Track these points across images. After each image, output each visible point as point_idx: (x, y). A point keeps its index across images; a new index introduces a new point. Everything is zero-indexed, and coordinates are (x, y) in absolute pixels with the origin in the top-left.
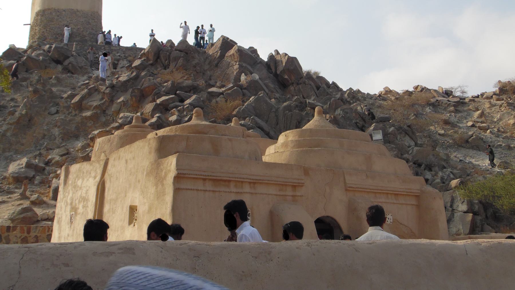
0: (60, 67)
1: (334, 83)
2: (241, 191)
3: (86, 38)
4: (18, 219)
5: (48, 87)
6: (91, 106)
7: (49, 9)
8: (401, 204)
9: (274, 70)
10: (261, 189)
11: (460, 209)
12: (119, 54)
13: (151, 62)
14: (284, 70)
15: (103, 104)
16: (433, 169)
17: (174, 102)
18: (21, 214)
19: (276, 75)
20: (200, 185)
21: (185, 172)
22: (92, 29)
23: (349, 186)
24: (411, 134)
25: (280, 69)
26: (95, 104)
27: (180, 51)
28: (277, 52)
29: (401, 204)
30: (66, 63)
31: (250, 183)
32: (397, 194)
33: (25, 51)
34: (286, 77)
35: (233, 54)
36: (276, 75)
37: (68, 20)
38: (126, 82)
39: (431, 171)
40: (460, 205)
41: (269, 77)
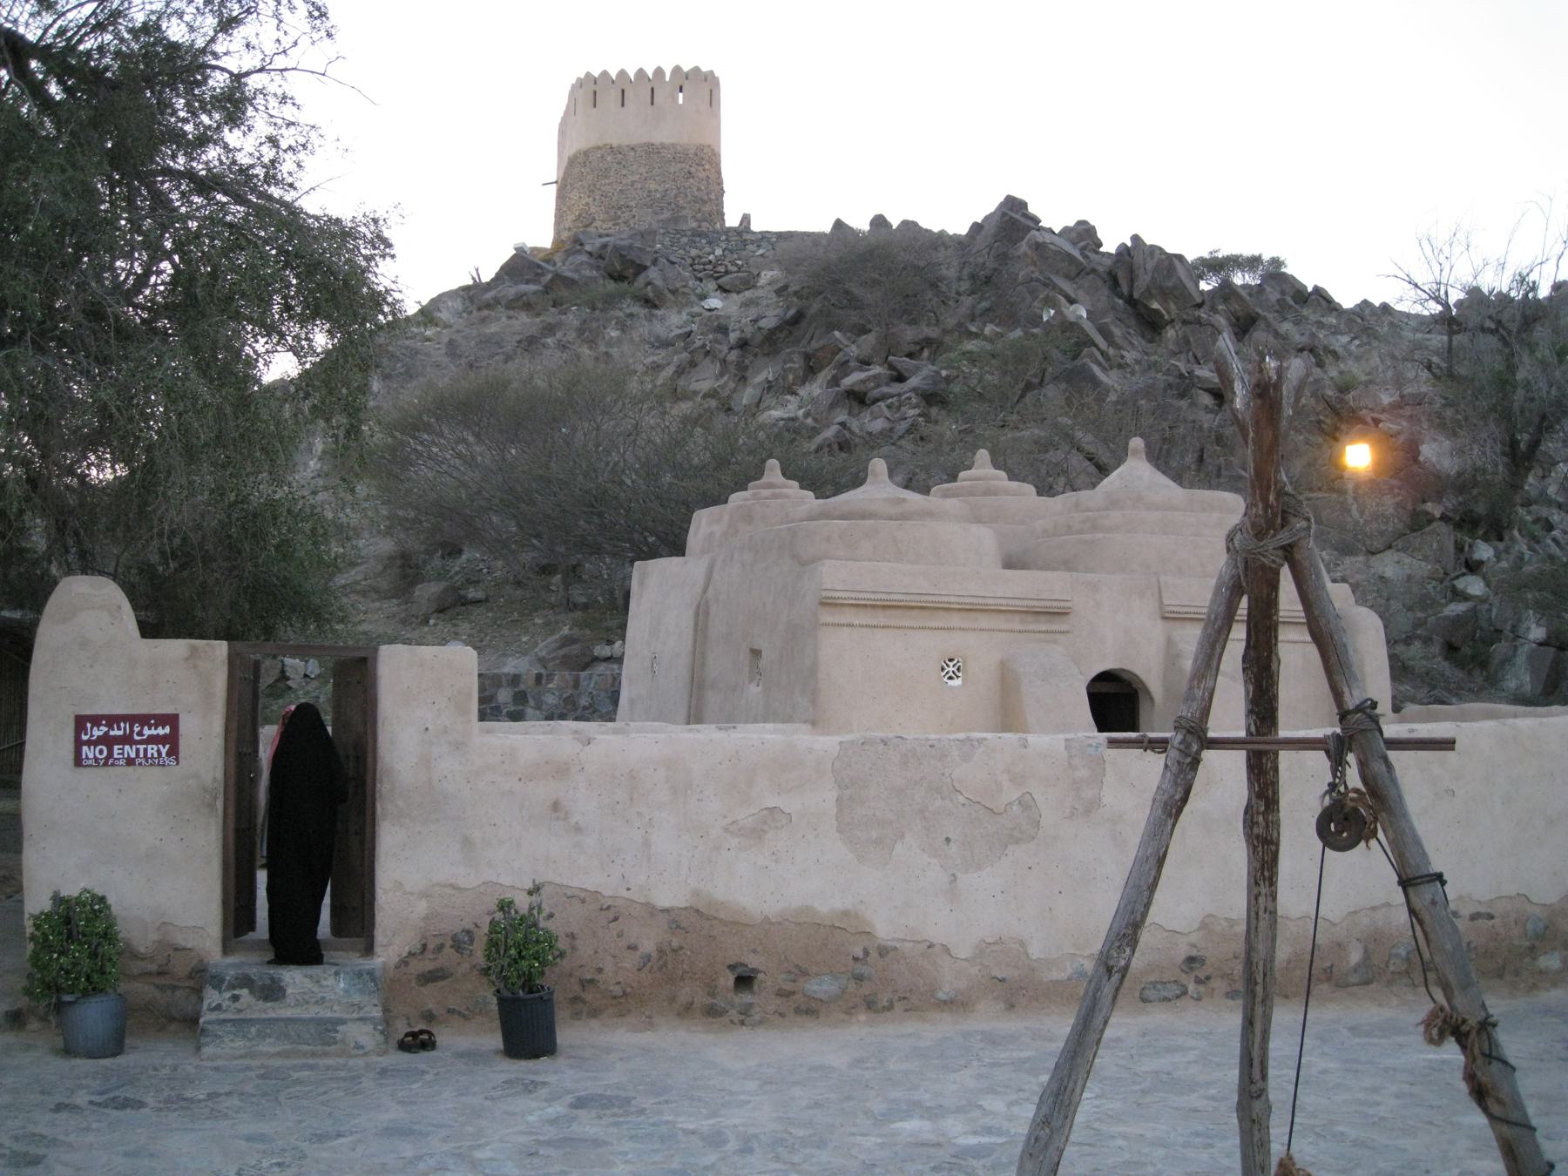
1: (1317, 290)
3: (684, 212)
4: (554, 659)
5: (603, 349)
6: (696, 393)
7: (598, 148)
9: (1125, 289)
11: (1532, 636)
12: (761, 252)
14: (1148, 289)
15: (722, 387)
17: (878, 386)
18: (560, 648)
19: (1131, 301)
21: (837, 594)
22: (699, 189)
25: (1143, 281)
26: (705, 386)
28: (1136, 239)
30: (641, 280)
33: (549, 256)
34: (1155, 306)
35: (1025, 254)
36: (1131, 301)
37: (642, 170)
38: (772, 331)
40: (1533, 626)
41: (1113, 308)
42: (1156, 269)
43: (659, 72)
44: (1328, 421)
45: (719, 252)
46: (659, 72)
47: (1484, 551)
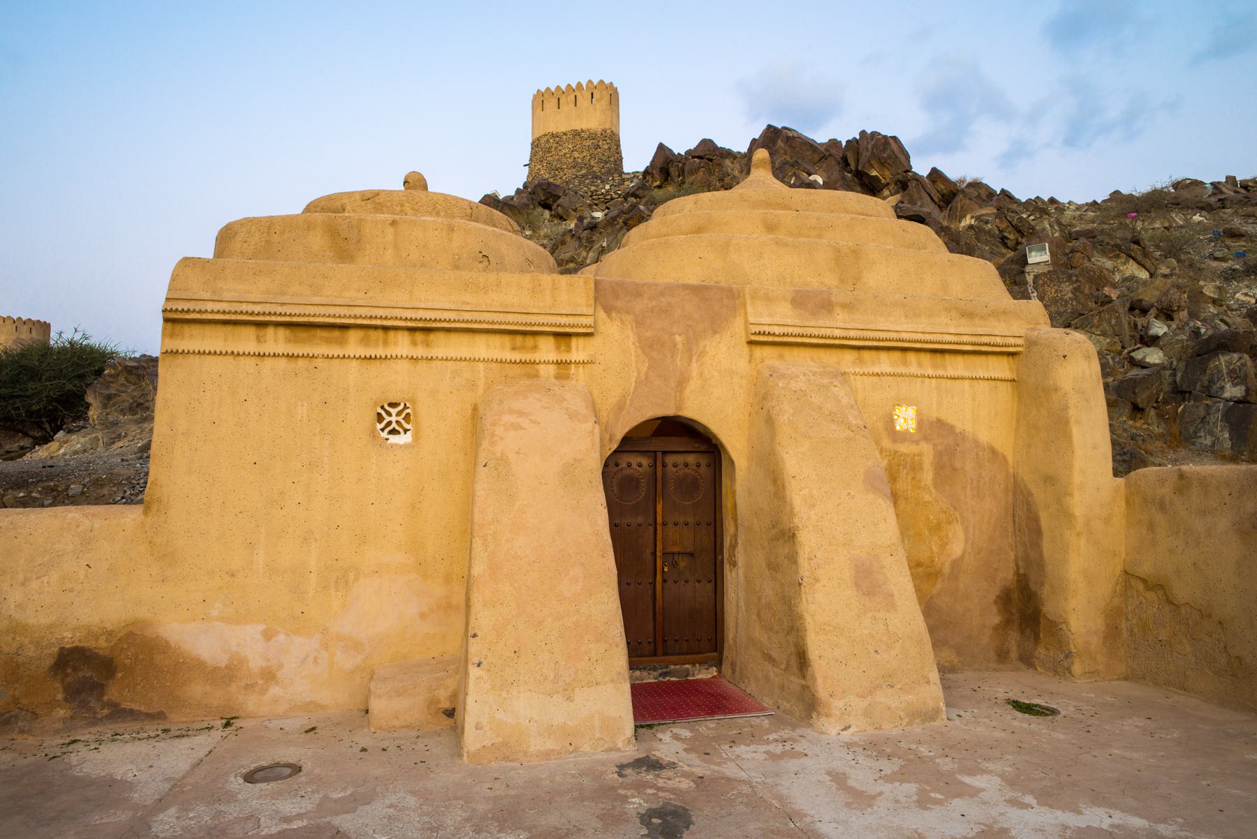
0: (547, 213)
2: (380, 352)
8: (951, 378)
9: (853, 166)
10: (444, 347)
11: (1227, 395)
13: (658, 183)
16: (1175, 316)
20: (246, 341)
23: (757, 329)
24: (1140, 258)
27: (700, 157)
29: (951, 378)
31: (412, 330)
32: (942, 352)
34: (874, 173)
39: (1172, 320)
42: (874, 146)
43: (579, 85)
44: (1011, 237)
45: (607, 187)
46: (579, 85)
47: (1159, 328)
